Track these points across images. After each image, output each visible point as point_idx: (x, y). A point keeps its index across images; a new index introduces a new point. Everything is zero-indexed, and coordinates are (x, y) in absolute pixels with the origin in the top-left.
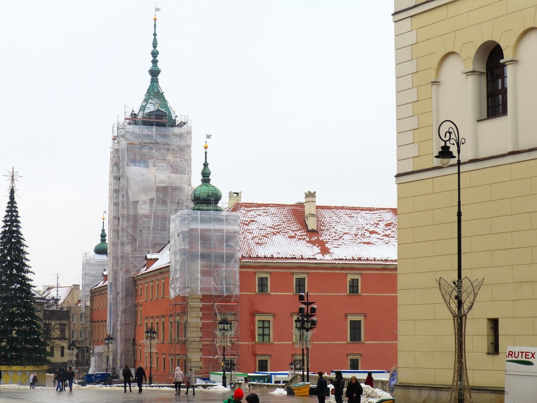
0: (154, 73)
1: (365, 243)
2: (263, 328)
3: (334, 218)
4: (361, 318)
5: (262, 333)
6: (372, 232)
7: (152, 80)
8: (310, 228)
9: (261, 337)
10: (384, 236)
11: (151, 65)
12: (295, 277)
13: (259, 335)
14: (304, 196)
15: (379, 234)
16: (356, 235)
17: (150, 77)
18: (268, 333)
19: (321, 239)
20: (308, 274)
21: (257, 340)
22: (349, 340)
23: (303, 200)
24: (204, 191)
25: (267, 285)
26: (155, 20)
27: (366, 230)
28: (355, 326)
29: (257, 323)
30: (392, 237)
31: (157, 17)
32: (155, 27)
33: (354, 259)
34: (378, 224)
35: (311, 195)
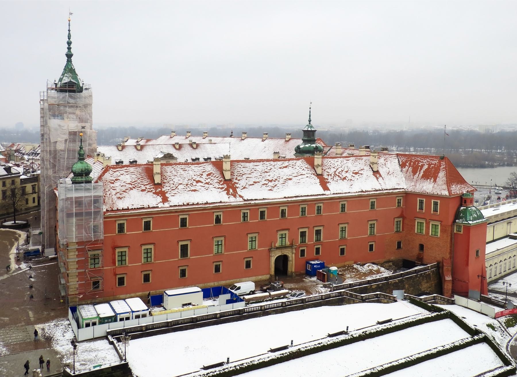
0: (69, 56)
1: (192, 191)
2: (122, 256)
3: (173, 172)
4: (188, 243)
6: (198, 182)
8: (156, 182)
10: (205, 183)
15: (202, 183)
16: (187, 185)
19: (163, 190)
20: (152, 218)
21: (117, 265)
26: (69, 21)
27: (194, 180)
28: (184, 248)
30: (211, 184)
32: (69, 25)
33: (184, 205)
34: (202, 175)
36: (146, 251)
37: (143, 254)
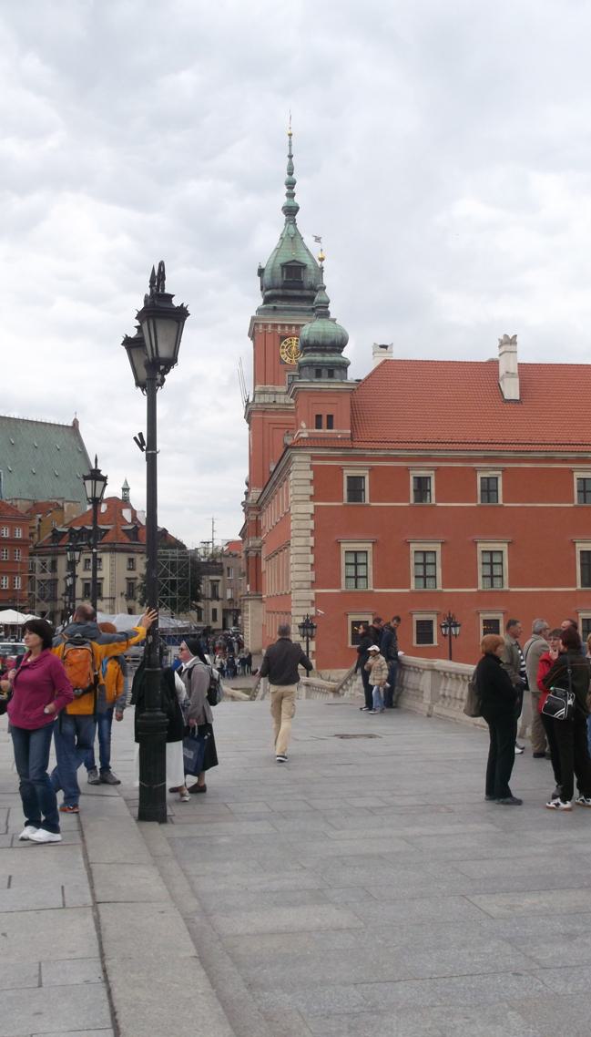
2: (425, 564)
5: (422, 574)
7: (286, 221)
9: (422, 580)
11: (286, 198)
12: (480, 475)
13: (416, 577)
14: (498, 344)
17: (284, 217)
18: (434, 574)
22: (579, 587)
23: (495, 356)
24: (317, 330)
25: (430, 491)
26: (290, 135)
29: (412, 555)
31: (292, 131)
32: (290, 146)
35: (509, 342)
36: (487, 559)
37: (480, 566)
